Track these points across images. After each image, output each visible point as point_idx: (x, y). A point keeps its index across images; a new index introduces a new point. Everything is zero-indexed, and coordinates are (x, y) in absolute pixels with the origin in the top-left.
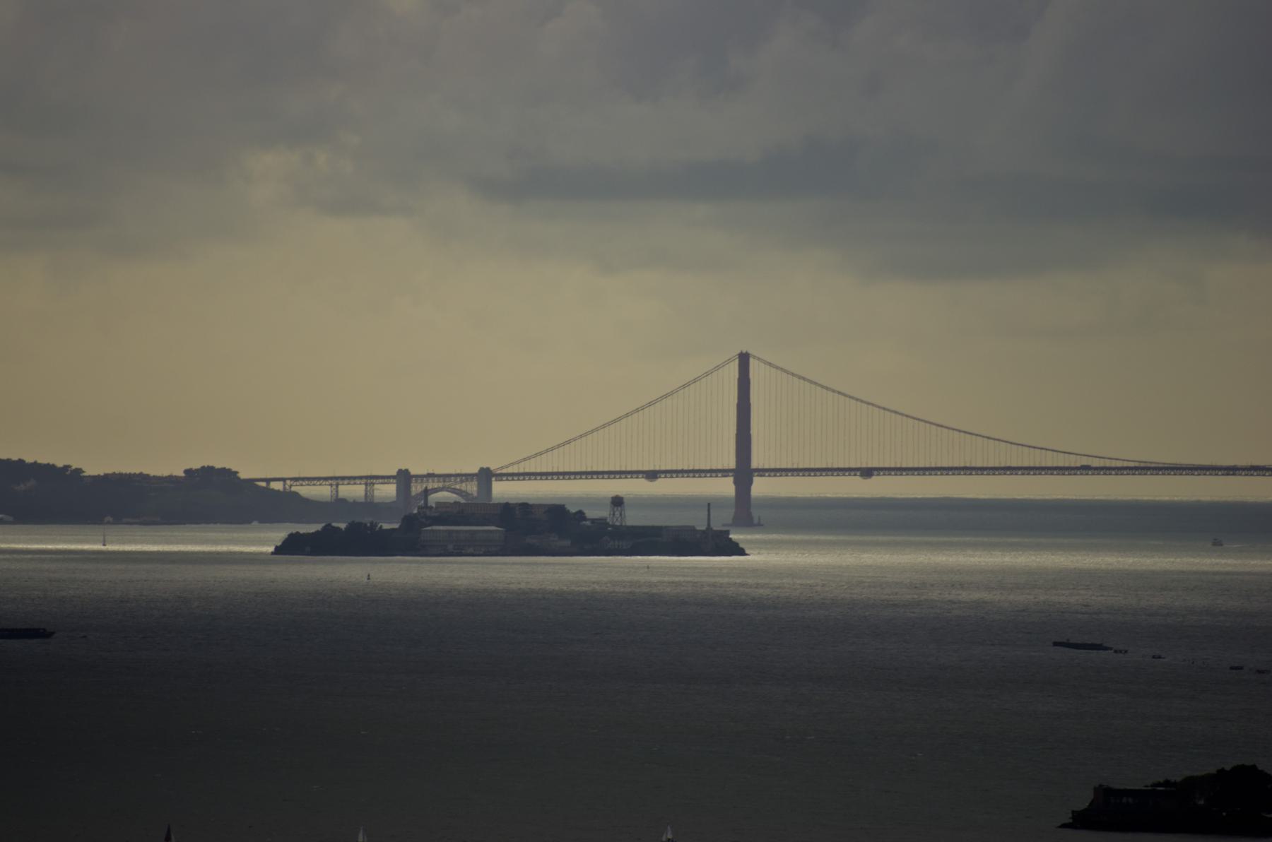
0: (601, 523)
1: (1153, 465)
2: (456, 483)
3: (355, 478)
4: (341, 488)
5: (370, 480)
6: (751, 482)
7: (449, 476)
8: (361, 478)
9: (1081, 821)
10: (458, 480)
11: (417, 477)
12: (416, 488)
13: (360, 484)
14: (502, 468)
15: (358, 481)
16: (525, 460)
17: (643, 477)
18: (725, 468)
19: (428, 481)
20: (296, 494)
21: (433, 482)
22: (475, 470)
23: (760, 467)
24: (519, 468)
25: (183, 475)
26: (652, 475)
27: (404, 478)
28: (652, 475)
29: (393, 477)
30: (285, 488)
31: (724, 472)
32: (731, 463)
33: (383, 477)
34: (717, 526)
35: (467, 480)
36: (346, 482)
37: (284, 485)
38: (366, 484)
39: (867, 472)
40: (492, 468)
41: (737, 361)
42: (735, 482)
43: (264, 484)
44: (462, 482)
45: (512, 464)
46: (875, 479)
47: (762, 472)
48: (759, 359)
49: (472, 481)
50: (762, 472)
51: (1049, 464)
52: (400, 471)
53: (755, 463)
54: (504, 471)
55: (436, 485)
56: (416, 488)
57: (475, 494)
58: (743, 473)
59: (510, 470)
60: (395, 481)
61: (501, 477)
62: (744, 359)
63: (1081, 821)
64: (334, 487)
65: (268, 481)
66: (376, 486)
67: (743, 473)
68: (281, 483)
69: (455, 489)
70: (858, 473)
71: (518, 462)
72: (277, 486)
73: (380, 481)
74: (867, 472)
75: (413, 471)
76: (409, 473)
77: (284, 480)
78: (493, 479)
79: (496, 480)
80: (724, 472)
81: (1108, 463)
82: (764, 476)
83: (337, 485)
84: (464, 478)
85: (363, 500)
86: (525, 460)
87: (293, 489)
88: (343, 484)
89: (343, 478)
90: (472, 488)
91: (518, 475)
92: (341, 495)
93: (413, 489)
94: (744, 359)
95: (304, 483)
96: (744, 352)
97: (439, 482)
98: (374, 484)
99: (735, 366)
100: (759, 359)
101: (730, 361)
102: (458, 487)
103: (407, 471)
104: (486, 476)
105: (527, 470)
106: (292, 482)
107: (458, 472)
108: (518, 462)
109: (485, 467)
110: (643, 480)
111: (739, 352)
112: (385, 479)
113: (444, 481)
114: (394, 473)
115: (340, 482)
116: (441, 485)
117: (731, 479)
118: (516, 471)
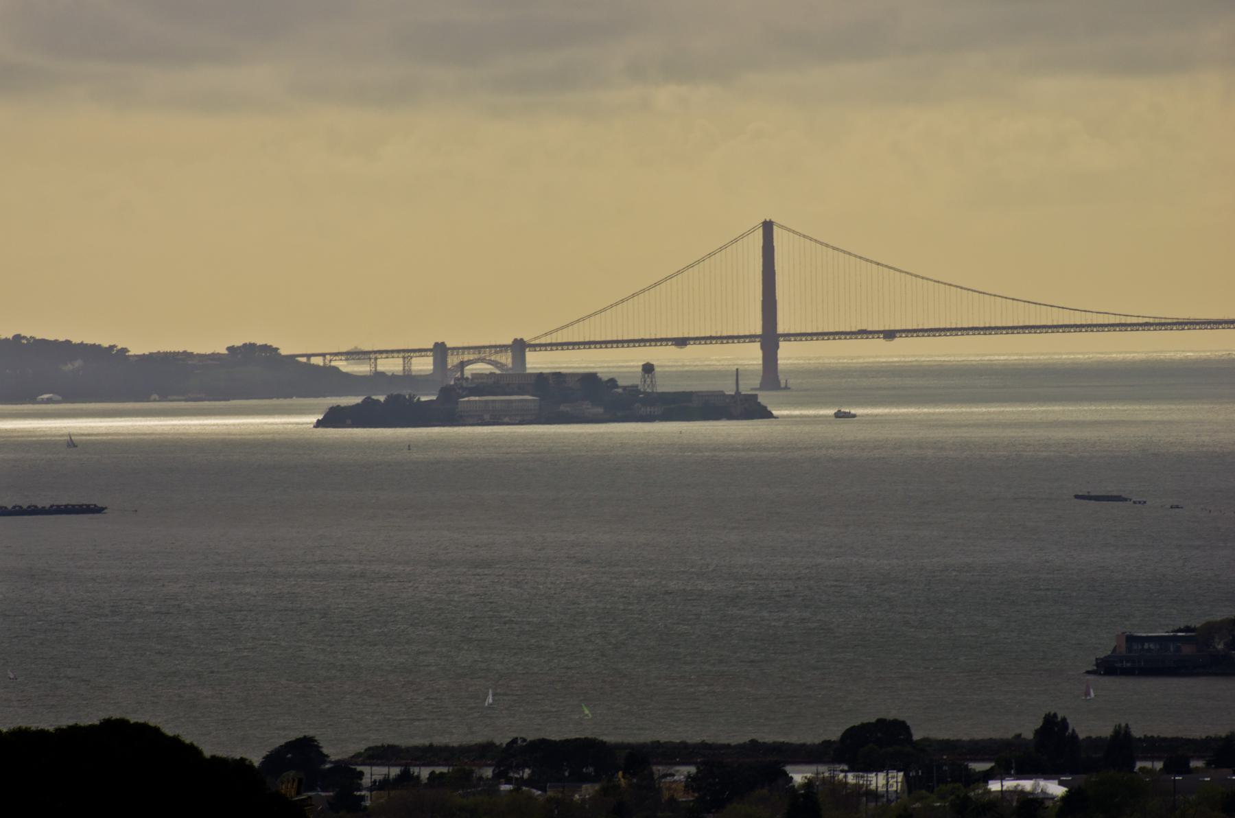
0: (633, 391)
1: (1169, 321)
2: (490, 354)
3: (392, 351)
4: (379, 361)
5: (407, 353)
6: (778, 347)
7: (484, 347)
8: (398, 351)
9: (1108, 667)
10: (493, 352)
11: (450, 349)
12: (452, 361)
13: (398, 357)
14: (535, 338)
15: (396, 355)
16: (557, 330)
17: (672, 345)
18: (751, 333)
19: (463, 353)
20: (336, 369)
21: (469, 354)
22: (509, 341)
23: (786, 332)
24: (552, 339)
25: (226, 352)
26: (681, 342)
27: (440, 350)
28: (681, 342)
30: (324, 363)
31: (751, 338)
32: (758, 329)
34: (745, 390)
35: (501, 351)
36: (384, 355)
37: (324, 360)
38: (404, 358)
39: (890, 335)
40: (526, 339)
41: (761, 229)
42: (762, 348)
43: (304, 360)
44: (496, 352)
45: (546, 334)
46: (897, 340)
47: (788, 337)
48: (782, 227)
49: (506, 351)
50: (788, 337)
51: (1067, 322)
52: (436, 344)
53: (781, 329)
54: (537, 342)
55: (471, 357)
56: (452, 361)
57: (510, 366)
58: (770, 339)
59: (543, 341)
60: (431, 354)
61: (534, 347)
62: (768, 227)
63: (1108, 667)
64: (373, 361)
65: (309, 356)
66: (414, 359)
67: (770, 339)
69: (490, 360)
70: (882, 336)
71: (551, 333)
72: (318, 361)
73: (417, 354)
74: (890, 335)
75: (449, 345)
76: (445, 345)
77: (324, 355)
78: (527, 350)
79: (530, 351)
80: (751, 338)
81: (1123, 320)
82: (790, 340)
84: (498, 349)
85: (401, 374)
86: (557, 330)
87: (333, 364)
88: (382, 358)
90: (506, 359)
91: (551, 345)
92: (380, 368)
93: (449, 361)
96: (768, 220)
97: (474, 353)
98: (411, 358)
99: (759, 234)
100: (782, 227)
101: (754, 229)
102: (493, 358)
103: (443, 344)
104: (520, 347)
105: (559, 341)
107: (493, 343)
108: (551, 333)
109: (519, 338)
110: (673, 347)
111: (763, 220)
112: (421, 351)
113: (480, 353)
116: (476, 356)
117: (758, 345)
118: (549, 341)
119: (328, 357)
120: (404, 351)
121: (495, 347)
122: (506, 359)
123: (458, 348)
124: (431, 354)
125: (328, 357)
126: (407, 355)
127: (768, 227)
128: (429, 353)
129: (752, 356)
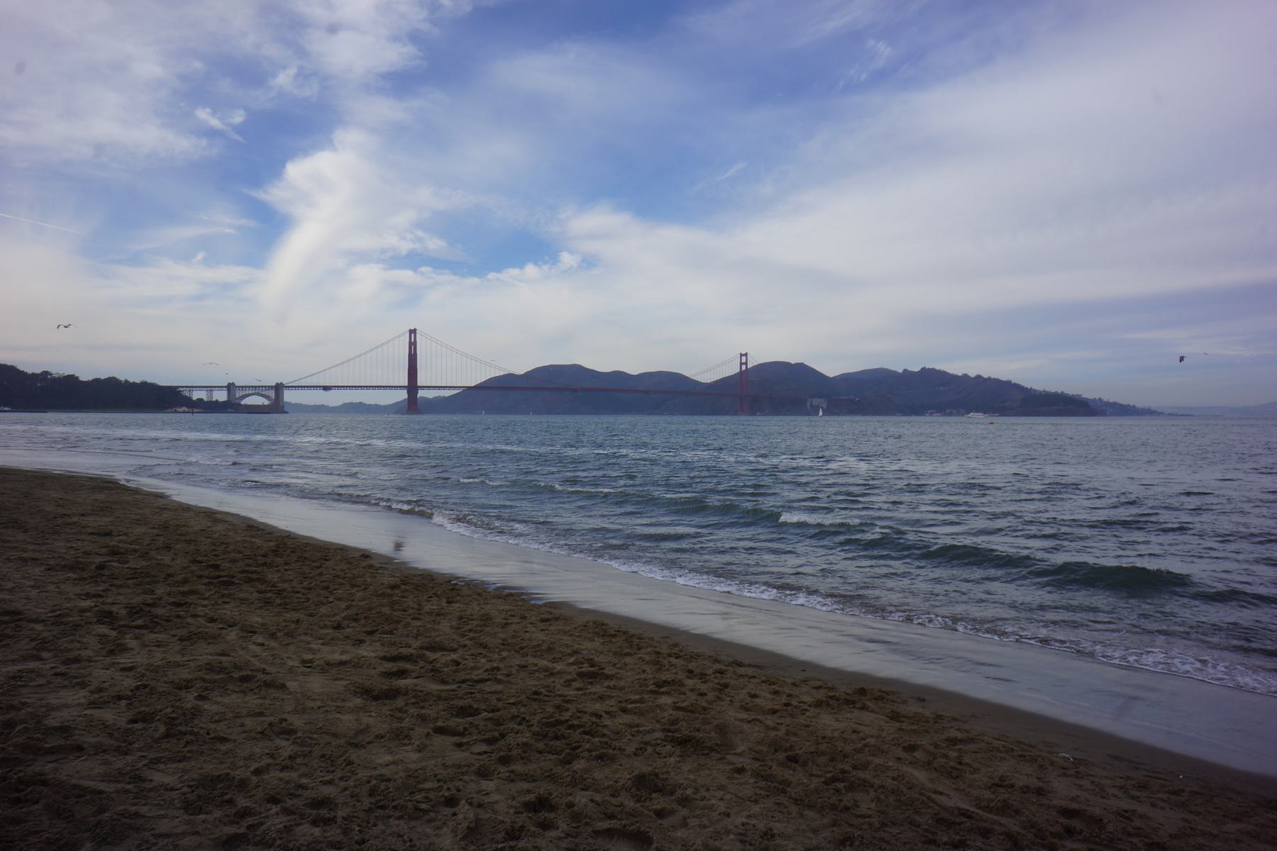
5: (210, 388)
11: (239, 387)
12: (239, 394)
27: (230, 387)
33: (219, 387)
42: (408, 393)
50: (423, 387)
53: (420, 383)
56: (239, 394)
58: (412, 387)
62: (413, 332)
67: (412, 387)
94: (413, 332)
101: (404, 333)
103: (233, 383)
104: (279, 388)
114: (226, 385)
121: (265, 387)
122: (272, 394)
123: (242, 387)
129: (403, 395)
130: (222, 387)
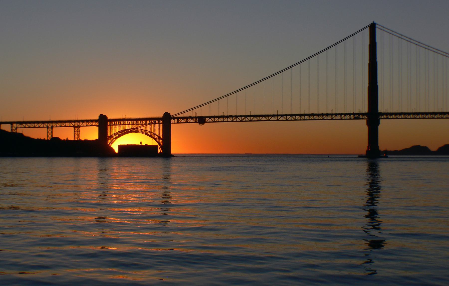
6: (378, 123)
11: (111, 120)
13: (70, 126)
15: (68, 124)
20: (21, 135)
29: (96, 121)
30: (12, 130)
31: (357, 116)
33: (88, 121)
36: (59, 125)
37: (12, 127)
44: (146, 124)
50: (388, 115)
53: (381, 109)
54: (180, 116)
56: (112, 130)
68: (9, 125)
71: (191, 109)
72: (7, 128)
73: (85, 124)
75: (109, 117)
77: (11, 123)
80: (357, 116)
83: (52, 127)
87: (19, 131)
88: (57, 127)
89: (83, 121)
95: (27, 126)
103: (105, 116)
106: (18, 125)
108: (191, 109)
115: (54, 125)
119: (15, 125)
120: (75, 121)
124: (98, 125)
125: (15, 125)
126: (76, 124)
127: (373, 27)
128: (94, 123)
130: (92, 121)
